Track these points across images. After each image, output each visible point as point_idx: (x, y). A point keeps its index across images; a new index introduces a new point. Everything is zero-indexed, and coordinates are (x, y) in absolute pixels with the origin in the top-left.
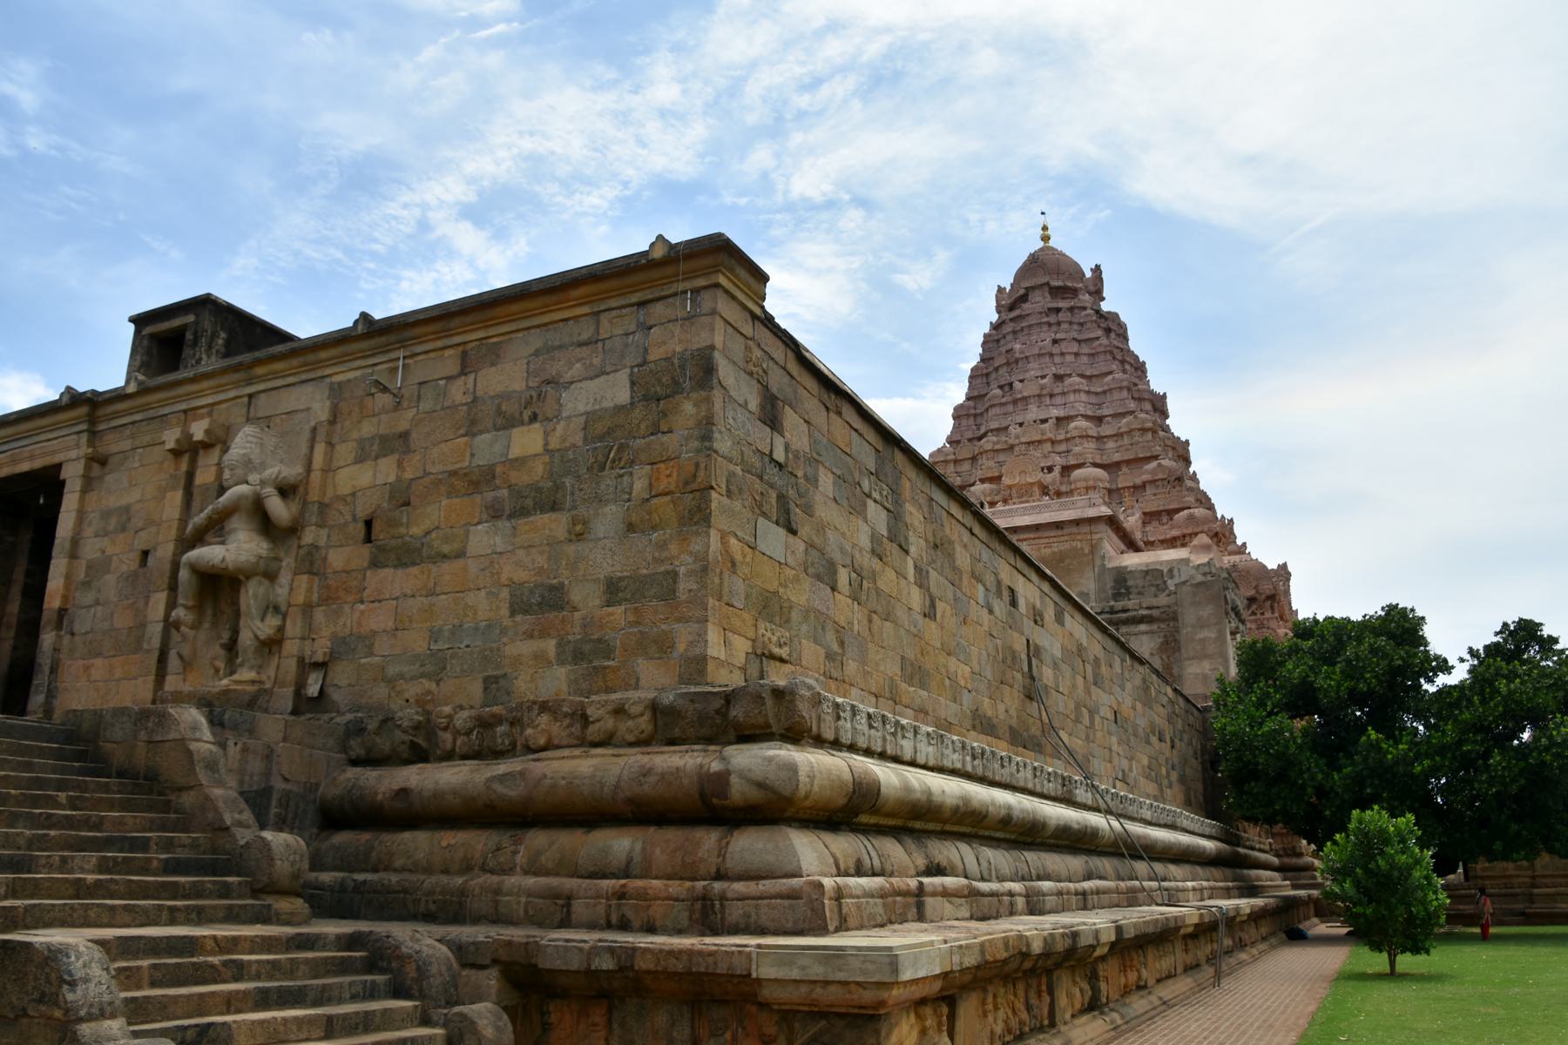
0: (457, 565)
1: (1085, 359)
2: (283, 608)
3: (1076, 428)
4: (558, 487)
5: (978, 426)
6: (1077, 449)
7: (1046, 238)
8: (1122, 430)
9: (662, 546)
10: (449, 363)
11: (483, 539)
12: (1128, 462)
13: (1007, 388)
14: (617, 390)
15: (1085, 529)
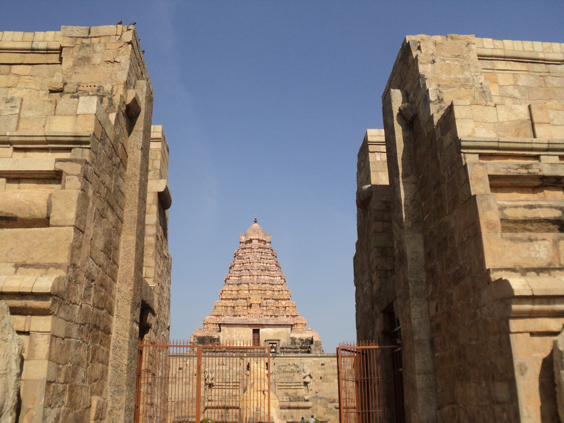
1: (268, 265)
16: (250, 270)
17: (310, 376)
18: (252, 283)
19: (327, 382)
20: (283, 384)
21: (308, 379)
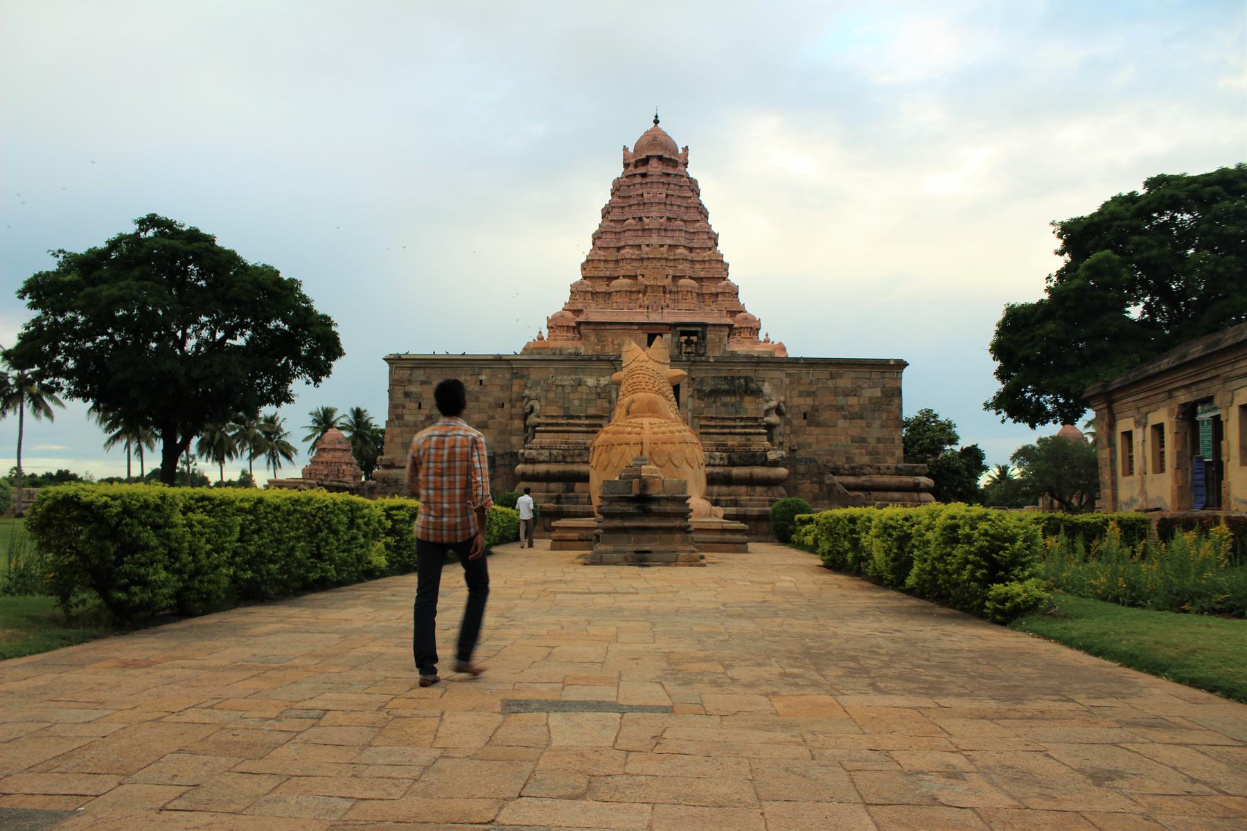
0: (835, 429)
1: (683, 210)
2: (782, 433)
3: (681, 254)
4: (862, 414)
5: (618, 240)
6: (680, 267)
7: (656, 122)
8: (705, 259)
9: (891, 431)
10: (826, 375)
11: (841, 423)
12: (708, 278)
13: (637, 220)
14: (877, 393)
15: (717, 328)
16: (644, 219)
17: (778, 411)
18: (648, 245)
19: (818, 425)
20: (713, 423)
21: (773, 419)
